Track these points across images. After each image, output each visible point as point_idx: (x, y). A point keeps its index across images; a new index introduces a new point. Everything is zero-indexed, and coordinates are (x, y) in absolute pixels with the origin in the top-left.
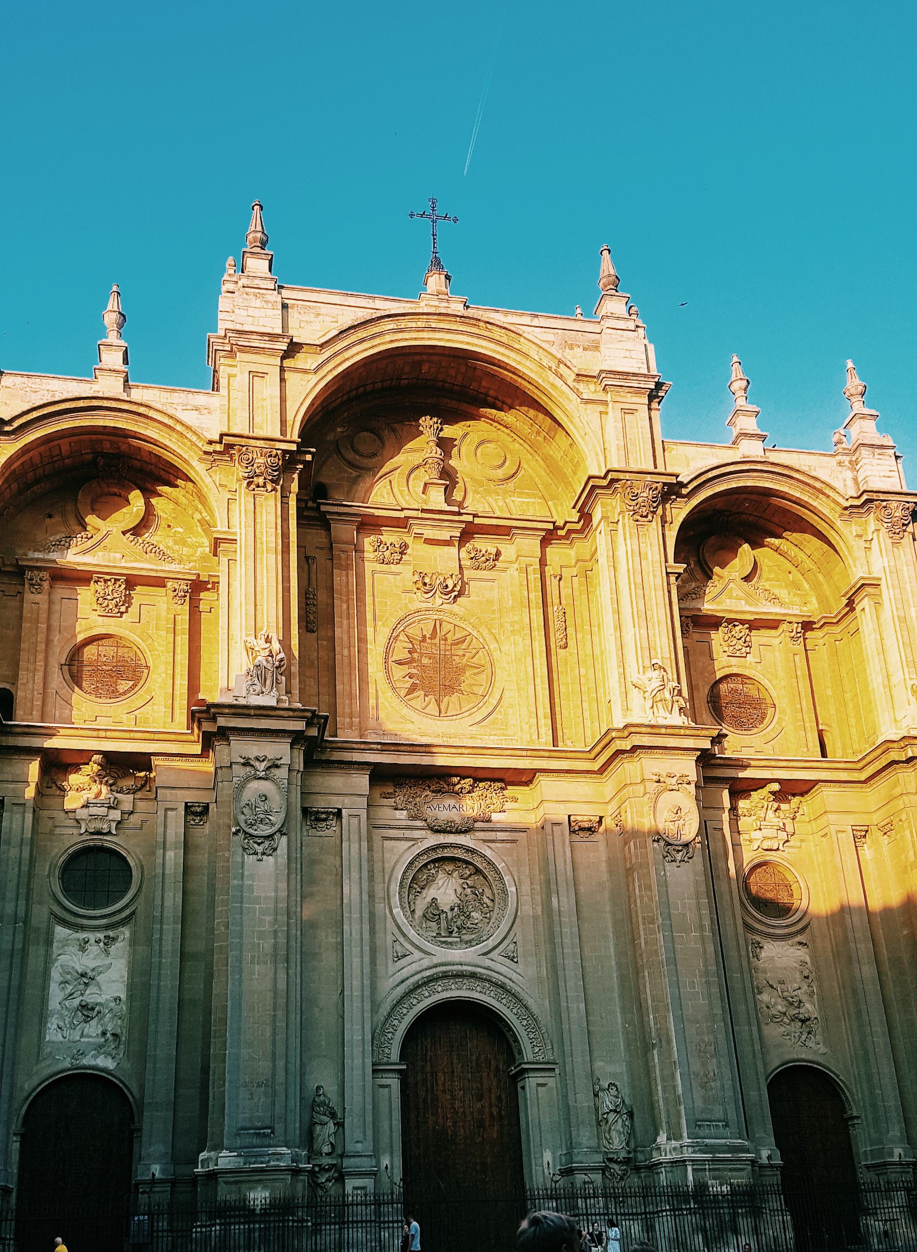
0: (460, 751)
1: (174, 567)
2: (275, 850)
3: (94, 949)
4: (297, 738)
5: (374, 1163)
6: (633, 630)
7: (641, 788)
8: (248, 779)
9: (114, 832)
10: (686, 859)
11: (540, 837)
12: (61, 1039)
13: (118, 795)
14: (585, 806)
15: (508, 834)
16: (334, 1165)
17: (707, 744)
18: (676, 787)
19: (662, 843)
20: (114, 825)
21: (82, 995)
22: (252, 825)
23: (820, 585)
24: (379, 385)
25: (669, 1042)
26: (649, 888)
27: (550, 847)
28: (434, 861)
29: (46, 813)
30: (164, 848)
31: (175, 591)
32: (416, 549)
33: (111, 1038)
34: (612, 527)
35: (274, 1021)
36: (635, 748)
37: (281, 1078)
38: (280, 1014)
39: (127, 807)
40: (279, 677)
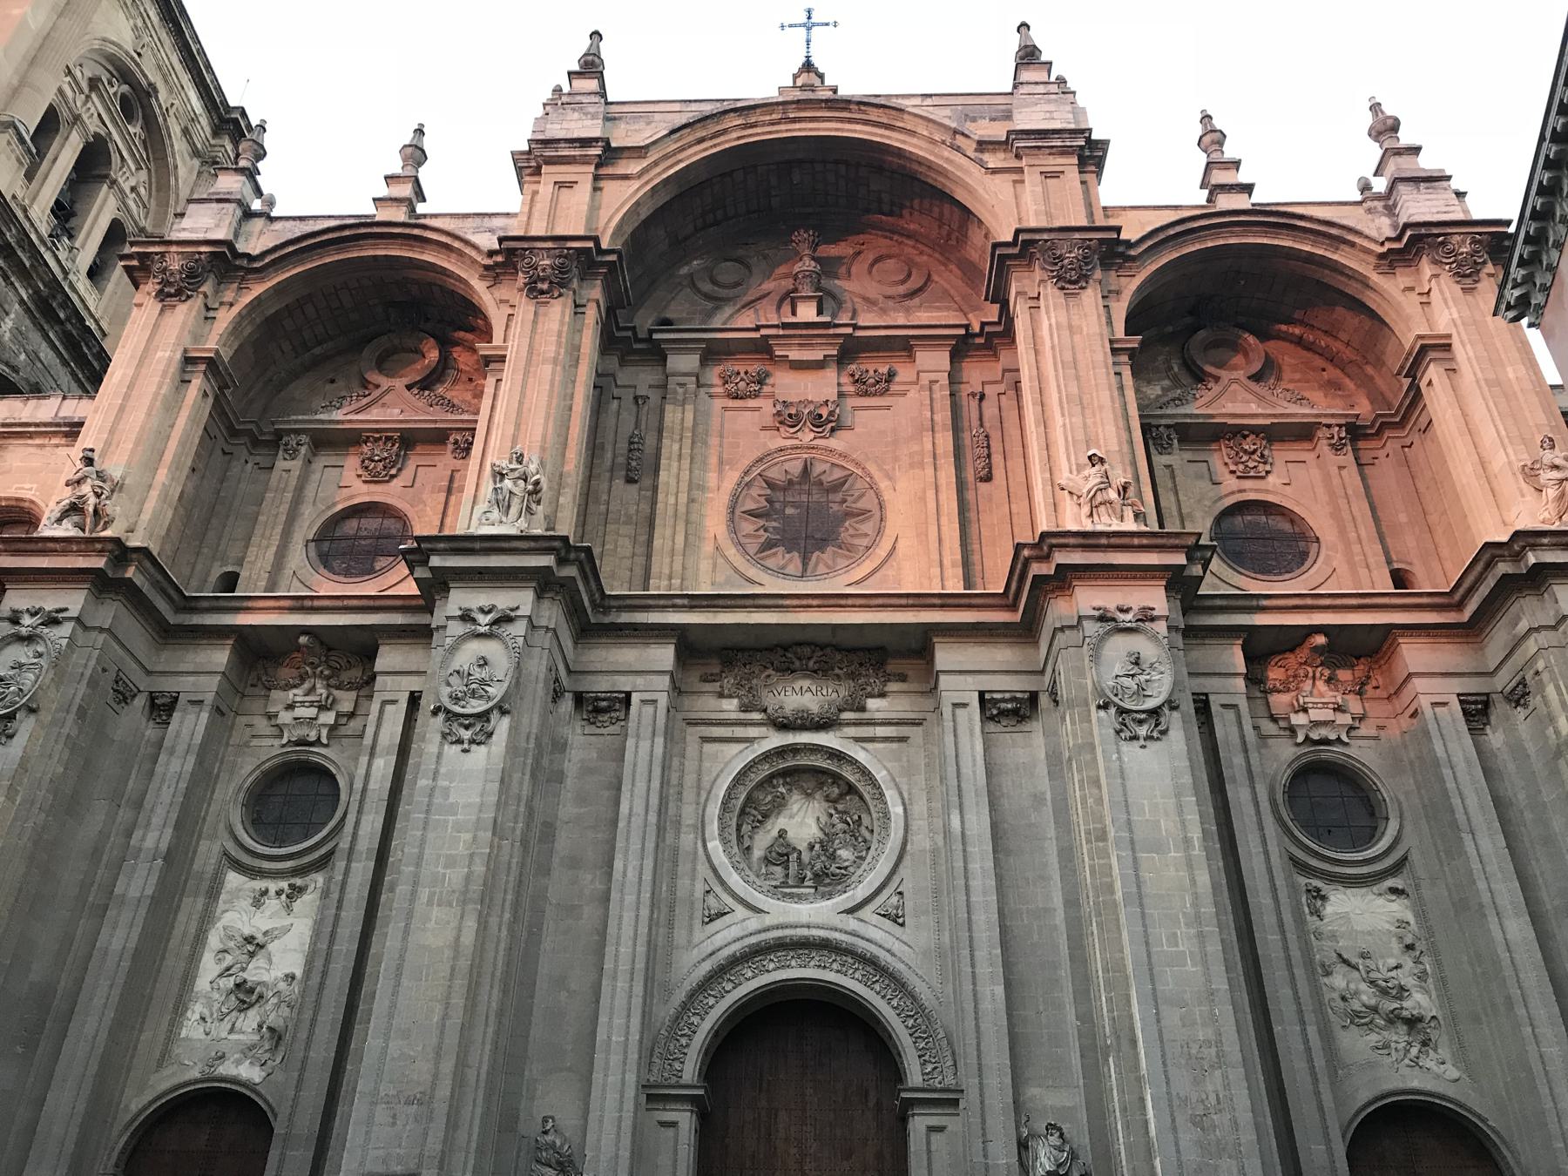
0: (804, 602)
1: (465, 417)
2: (490, 735)
3: (272, 904)
4: (544, 583)
9: (324, 741)
12: (203, 1036)
13: (336, 693)
14: (1007, 678)
17: (1181, 559)
19: (1113, 710)
20: (324, 732)
21: (243, 970)
22: (456, 699)
23: (1371, 378)
25: (1134, 1042)
26: (1096, 783)
28: (785, 773)
29: (242, 720)
30: (372, 755)
31: (456, 442)
33: (267, 1035)
35: (448, 997)
37: (444, 1091)
38: (460, 983)
39: (346, 706)
40: (534, 506)
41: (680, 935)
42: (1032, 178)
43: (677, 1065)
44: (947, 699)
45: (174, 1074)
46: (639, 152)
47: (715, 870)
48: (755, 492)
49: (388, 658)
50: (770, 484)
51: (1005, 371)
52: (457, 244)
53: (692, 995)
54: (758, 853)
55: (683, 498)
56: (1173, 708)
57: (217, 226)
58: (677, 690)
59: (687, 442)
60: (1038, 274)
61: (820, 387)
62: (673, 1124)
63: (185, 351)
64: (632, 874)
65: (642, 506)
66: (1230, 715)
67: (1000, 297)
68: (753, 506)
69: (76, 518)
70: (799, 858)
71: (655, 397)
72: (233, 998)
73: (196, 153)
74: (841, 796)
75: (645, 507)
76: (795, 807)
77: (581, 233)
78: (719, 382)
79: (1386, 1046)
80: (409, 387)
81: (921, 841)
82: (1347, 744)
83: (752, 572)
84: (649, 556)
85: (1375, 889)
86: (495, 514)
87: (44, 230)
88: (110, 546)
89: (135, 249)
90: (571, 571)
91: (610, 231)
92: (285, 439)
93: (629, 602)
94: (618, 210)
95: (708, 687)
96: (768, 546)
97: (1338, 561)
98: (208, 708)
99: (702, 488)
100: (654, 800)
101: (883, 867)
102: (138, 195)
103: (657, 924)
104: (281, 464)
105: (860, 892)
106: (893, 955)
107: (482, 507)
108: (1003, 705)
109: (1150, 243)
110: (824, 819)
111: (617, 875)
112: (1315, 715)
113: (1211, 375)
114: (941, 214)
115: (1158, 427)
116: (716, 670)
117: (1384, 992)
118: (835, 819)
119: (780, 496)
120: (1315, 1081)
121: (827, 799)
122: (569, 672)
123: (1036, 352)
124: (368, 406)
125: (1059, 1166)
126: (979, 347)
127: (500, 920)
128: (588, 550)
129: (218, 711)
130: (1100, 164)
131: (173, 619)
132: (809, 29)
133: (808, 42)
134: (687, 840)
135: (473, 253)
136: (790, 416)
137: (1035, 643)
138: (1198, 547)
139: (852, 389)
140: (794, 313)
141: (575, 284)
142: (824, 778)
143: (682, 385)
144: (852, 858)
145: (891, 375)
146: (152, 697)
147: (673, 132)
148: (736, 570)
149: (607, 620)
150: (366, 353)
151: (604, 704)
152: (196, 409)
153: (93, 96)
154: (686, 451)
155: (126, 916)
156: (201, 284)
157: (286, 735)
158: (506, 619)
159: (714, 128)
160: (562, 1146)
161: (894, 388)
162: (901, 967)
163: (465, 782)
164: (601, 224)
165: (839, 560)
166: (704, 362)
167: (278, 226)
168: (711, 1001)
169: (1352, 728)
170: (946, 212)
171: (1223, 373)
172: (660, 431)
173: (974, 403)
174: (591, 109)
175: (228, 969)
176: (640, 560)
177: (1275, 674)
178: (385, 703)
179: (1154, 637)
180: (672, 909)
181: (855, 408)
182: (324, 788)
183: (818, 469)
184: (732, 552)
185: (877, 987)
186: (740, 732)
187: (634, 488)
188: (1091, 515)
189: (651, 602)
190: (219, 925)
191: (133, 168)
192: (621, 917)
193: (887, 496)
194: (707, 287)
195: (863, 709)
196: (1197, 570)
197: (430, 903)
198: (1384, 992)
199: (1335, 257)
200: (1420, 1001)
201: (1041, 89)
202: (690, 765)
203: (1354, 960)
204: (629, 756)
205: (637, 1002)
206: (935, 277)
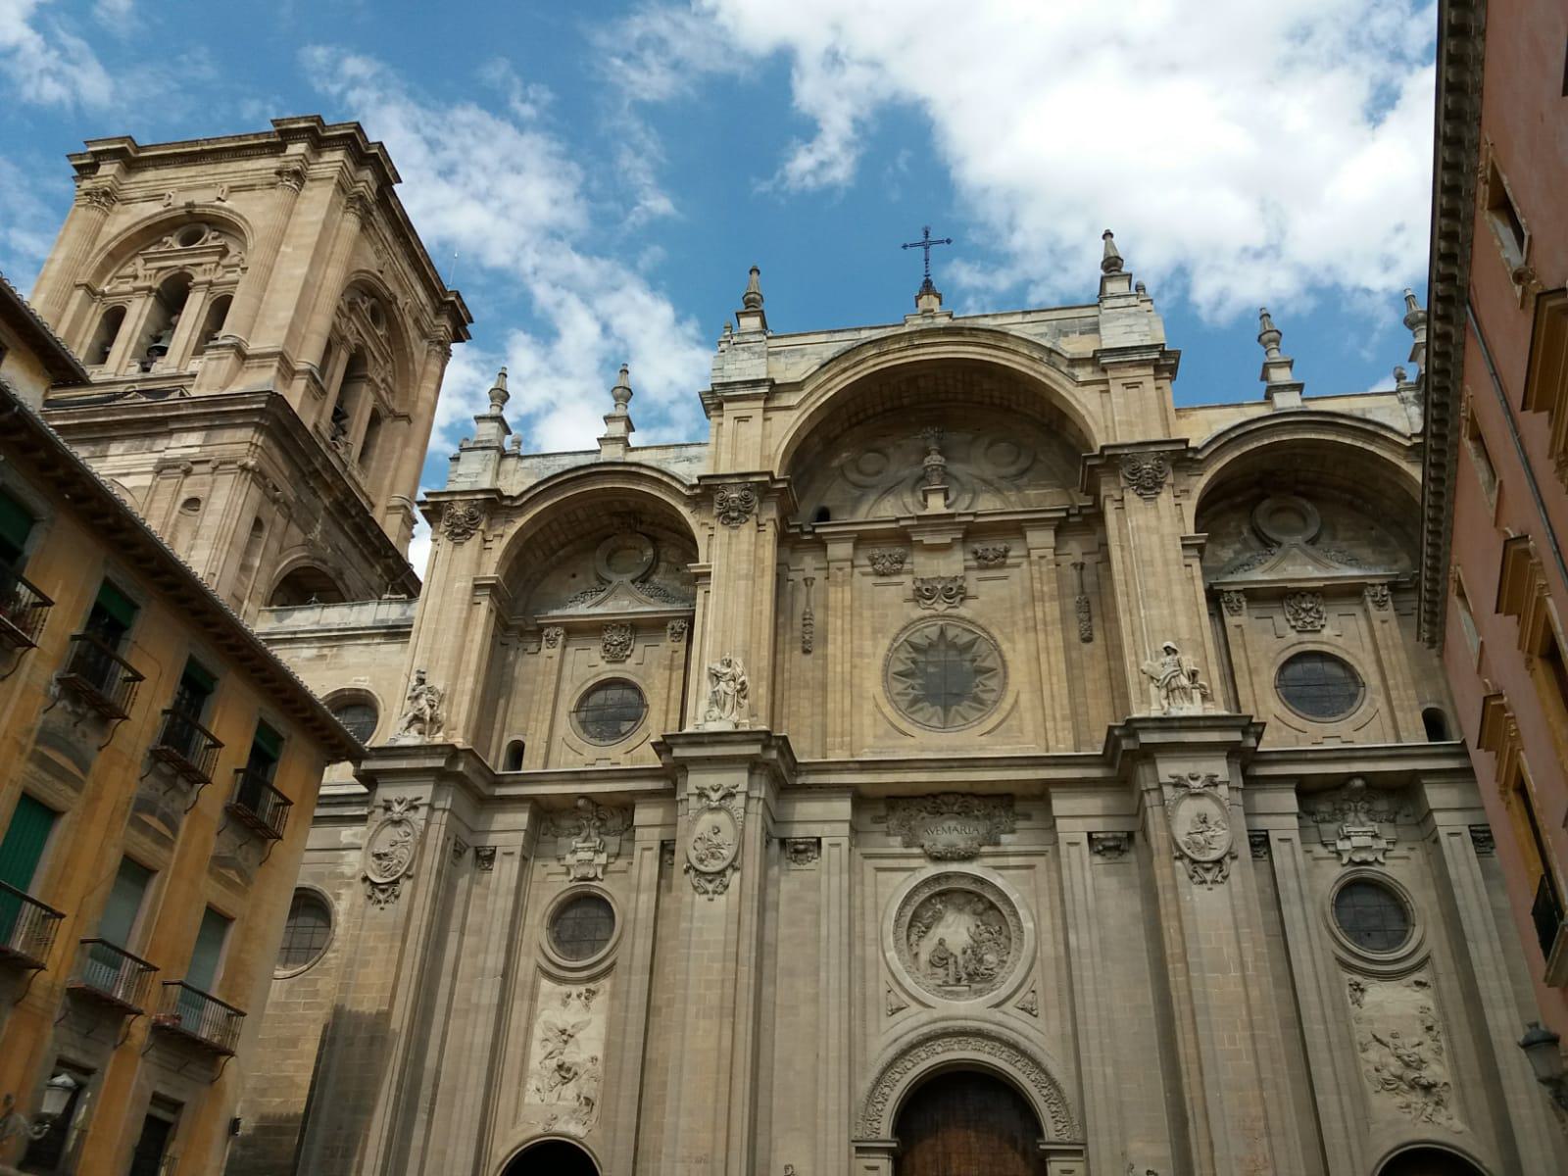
0: (948, 764)
2: (726, 887)
3: (575, 1003)
4: (753, 765)
8: (700, 812)
9: (600, 876)
10: (1219, 879)
13: (607, 838)
17: (1237, 736)
18: (1201, 791)
19: (1186, 861)
20: (599, 870)
21: (561, 1054)
24: (879, 409)
27: (1065, 872)
28: (940, 894)
30: (638, 891)
37: (721, 1155)
38: (724, 1077)
39: (613, 849)
40: (741, 701)
41: (871, 1028)
42: (1116, 388)
43: (875, 1124)
45: (523, 1131)
46: (796, 386)
49: (644, 815)
50: (915, 648)
51: (1100, 545)
52: (665, 479)
53: (884, 1072)
54: (924, 957)
55: (847, 666)
56: (1234, 858)
57: (484, 470)
58: (855, 831)
59: (848, 618)
60: (1123, 483)
61: (952, 565)
62: (876, 1168)
63: (475, 579)
66: (1286, 846)
67: (1092, 490)
68: (901, 668)
69: (419, 725)
70: (956, 962)
71: (820, 576)
72: (556, 1074)
73: (424, 335)
74: (985, 909)
75: (819, 674)
77: (757, 469)
79: (1408, 1106)
80: (633, 582)
82: (1383, 864)
83: (904, 726)
84: (825, 714)
85: (1404, 981)
86: (716, 711)
87: (329, 439)
88: (447, 750)
89: (429, 500)
91: (779, 457)
92: (545, 633)
93: (815, 767)
94: (784, 438)
95: (877, 827)
96: (915, 701)
97: (1380, 702)
98: (518, 858)
99: (861, 655)
100: (845, 924)
102: (387, 384)
104: (545, 651)
105: (1003, 991)
106: (1031, 1041)
107: (704, 704)
109: (1214, 446)
110: (973, 929)
111: (823, 983)
112: (1357, 841)
113: (1274, 541)
115: (1229, 592)
116: (883, 813)
117: (1408, 1065)
119: (921, 658)
120: (1347, 1137)
121: (975, 913)
122: (774, 822)
124: (605, 599)
127: (745, 1027)
128: (785, 739)
129: (524, 859)
130: (1173, 370)
131: (487, 791)
132: (927, 248)
133: (927, 260)
134: (871, 951)
135: (678, 486)
136: (927, 590)
137: (1131, 792)
138: (1251, 724)
139: (975, 564)
140: (926, 500)
141: (756, 510)
142: (971, 896)
143: (840, 569)
144: (996, 961)
145: (1007, 550)
146: (477, 852)
147: (823, 366)
148: (893, 725)
149: (800, 781)
150: (598, 553)
151: (802, 847)
152: (487, 622)
153: (353, 317)
154: (847, 626)
155: (482, 1018)
156: (477, 524)
157: (572, 871)
161: (1009, 561)
163: (710, 919)
164: (774, 449)
165: (975, 712)
166: (855, 548)
167: (527, 463)
168: (897, 1076)
169: (1387, 850)
171: (1286, 539)
172: (826, 607)
173: (1074, 573)
174: (757, 348)
175: (551, 1053)
176: (818, 719)
177: (1324, 808)
178: (644, 849)
179: (1217, 800)
181: (979, 580)
182: (602, 913)
183: (951, 633)
184: (887, 709)
185: (1019, 1064)
186: (904, 863)
187: (809, 657)
188: (1168, 697)
189: (831, 767)
190: (540, 1020)
191: (382, 363)
192: (828, 1016)
193: (1009, 656)
194: (854, 477)
195: (997, 844)
196: (1252, 742)
197: (697, 1016)
198: (1408, 1065)
199: (1372, 448)
200: (1436, 1071)
201: (1122, 302)
202: (869, 890)
203: (1386, 1039)
204: (823, 886)
205: (845, 1080)
206: (1042, 457)
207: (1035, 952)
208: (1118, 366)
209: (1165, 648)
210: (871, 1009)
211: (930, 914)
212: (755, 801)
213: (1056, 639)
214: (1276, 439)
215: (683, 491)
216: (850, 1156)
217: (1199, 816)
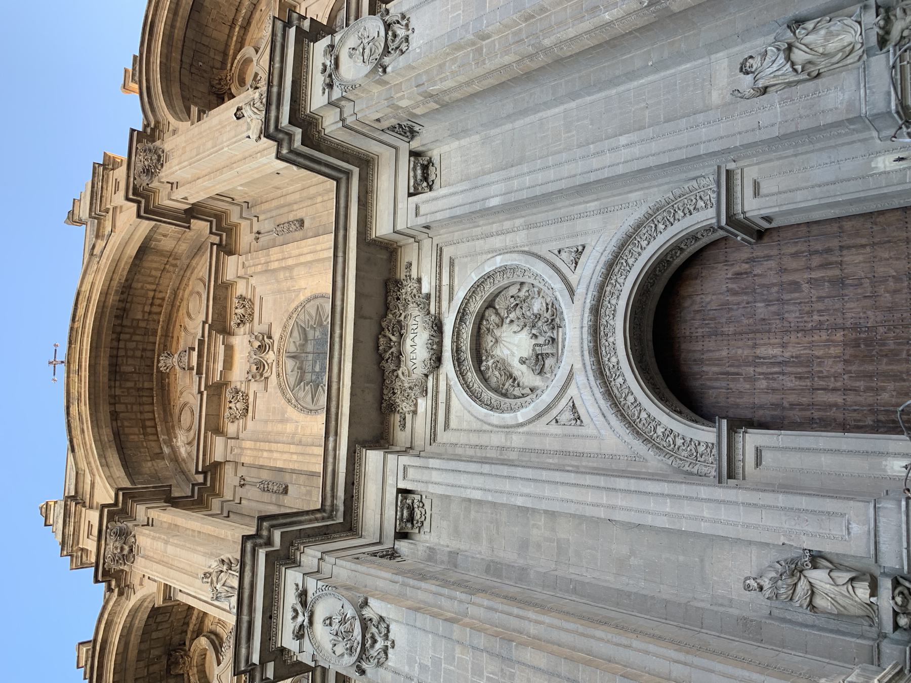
0: (337, 340)
2: (382, 619)
4: (284, 558)
5: (888, 505)
6: (226, 149)
7: (348, 109)
10: (404, 23)
11: (442, 231)
15: (444, 271)
16: (896, 583)
17: (292, 32)
19: (386, 60)
22: (351, 650)
27: (439, 216)
32: (238, 375)
34: (175, 186)
36: (294, 120)
41: (591, 446)
43: (701, 449)
44: (413, 221)
47: (540, 415)
48: (301, 394)
51: (241, 217)
52: (106, 616)
53: (638, 434)
54: (537, 381)
55: (293, 448)
62: (758, 452)
64: (529, 489)
65: (301, 482)
70: (540, 345)
71: (242, 471)
74: (497, 314)
75: (302, 478)
76: (506, 352)
78: (237, 422)
80: (219, 663)
81: (520, 238)
90: (277, 535)
93: (328, 488)
94: (108, 491)
101: (540, 268)
103: (577, 467)
105: (558, 285)
108: (419, 177)
110: (515, 327)
114: (156, 269)
118: (512, 316)
119: (308, 377)
121: (500, 325)
122: (380, 543)
123: (198, 178)
125: (778, 50)
126: (229, 236)
134: (517, 441)
142: (484, 328)
144: (540, 299)
145: (242, 298)
147: (73, 450)
149: (341, 508)
151: (405, 512)
158: (303, 595)
159: (76, 423)
160: (777, 572)
162: (614, 240)
168: (644, 415)
170: (155, 265)
180: (566, 454)
181: (260, 322)
185: (631, 261)
186: (442, 397)
189: (330, 469)
193: (308, 294)
195: (428, 296)
202: (463, 439)
205: (633, 484)
207: (524, 252)
208: (104, 199)
209: (238, 118)
210: (575, 445)
211: (497, 373)
212: (323, 564)
213: (292, 249)
214: (158, 69)
215: (114, 599)
216: (737, 487)
217: (351, 56)
